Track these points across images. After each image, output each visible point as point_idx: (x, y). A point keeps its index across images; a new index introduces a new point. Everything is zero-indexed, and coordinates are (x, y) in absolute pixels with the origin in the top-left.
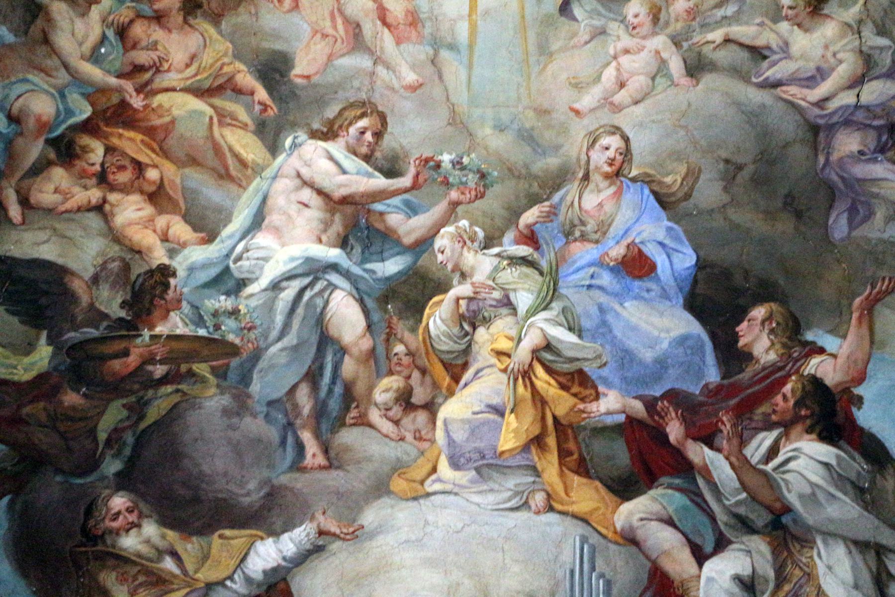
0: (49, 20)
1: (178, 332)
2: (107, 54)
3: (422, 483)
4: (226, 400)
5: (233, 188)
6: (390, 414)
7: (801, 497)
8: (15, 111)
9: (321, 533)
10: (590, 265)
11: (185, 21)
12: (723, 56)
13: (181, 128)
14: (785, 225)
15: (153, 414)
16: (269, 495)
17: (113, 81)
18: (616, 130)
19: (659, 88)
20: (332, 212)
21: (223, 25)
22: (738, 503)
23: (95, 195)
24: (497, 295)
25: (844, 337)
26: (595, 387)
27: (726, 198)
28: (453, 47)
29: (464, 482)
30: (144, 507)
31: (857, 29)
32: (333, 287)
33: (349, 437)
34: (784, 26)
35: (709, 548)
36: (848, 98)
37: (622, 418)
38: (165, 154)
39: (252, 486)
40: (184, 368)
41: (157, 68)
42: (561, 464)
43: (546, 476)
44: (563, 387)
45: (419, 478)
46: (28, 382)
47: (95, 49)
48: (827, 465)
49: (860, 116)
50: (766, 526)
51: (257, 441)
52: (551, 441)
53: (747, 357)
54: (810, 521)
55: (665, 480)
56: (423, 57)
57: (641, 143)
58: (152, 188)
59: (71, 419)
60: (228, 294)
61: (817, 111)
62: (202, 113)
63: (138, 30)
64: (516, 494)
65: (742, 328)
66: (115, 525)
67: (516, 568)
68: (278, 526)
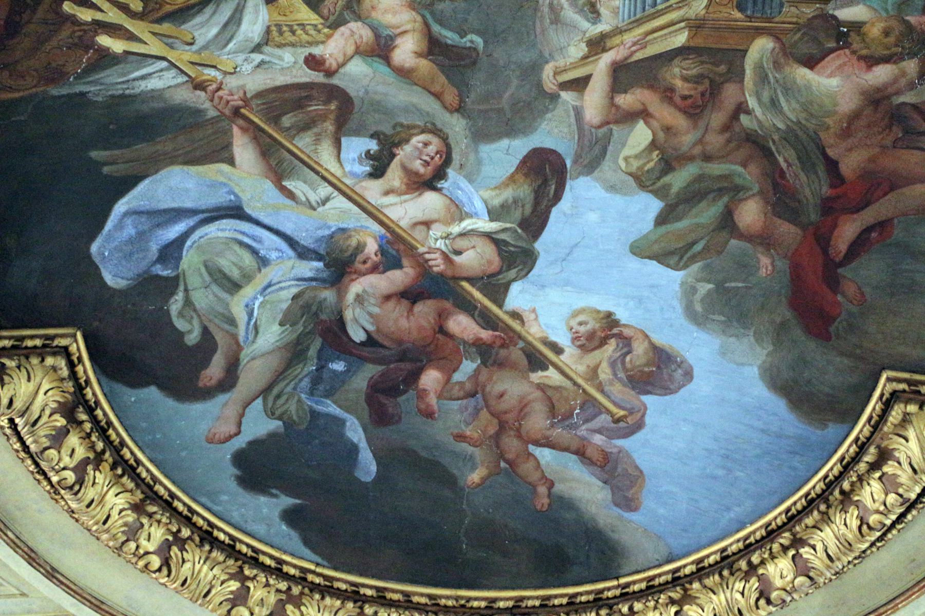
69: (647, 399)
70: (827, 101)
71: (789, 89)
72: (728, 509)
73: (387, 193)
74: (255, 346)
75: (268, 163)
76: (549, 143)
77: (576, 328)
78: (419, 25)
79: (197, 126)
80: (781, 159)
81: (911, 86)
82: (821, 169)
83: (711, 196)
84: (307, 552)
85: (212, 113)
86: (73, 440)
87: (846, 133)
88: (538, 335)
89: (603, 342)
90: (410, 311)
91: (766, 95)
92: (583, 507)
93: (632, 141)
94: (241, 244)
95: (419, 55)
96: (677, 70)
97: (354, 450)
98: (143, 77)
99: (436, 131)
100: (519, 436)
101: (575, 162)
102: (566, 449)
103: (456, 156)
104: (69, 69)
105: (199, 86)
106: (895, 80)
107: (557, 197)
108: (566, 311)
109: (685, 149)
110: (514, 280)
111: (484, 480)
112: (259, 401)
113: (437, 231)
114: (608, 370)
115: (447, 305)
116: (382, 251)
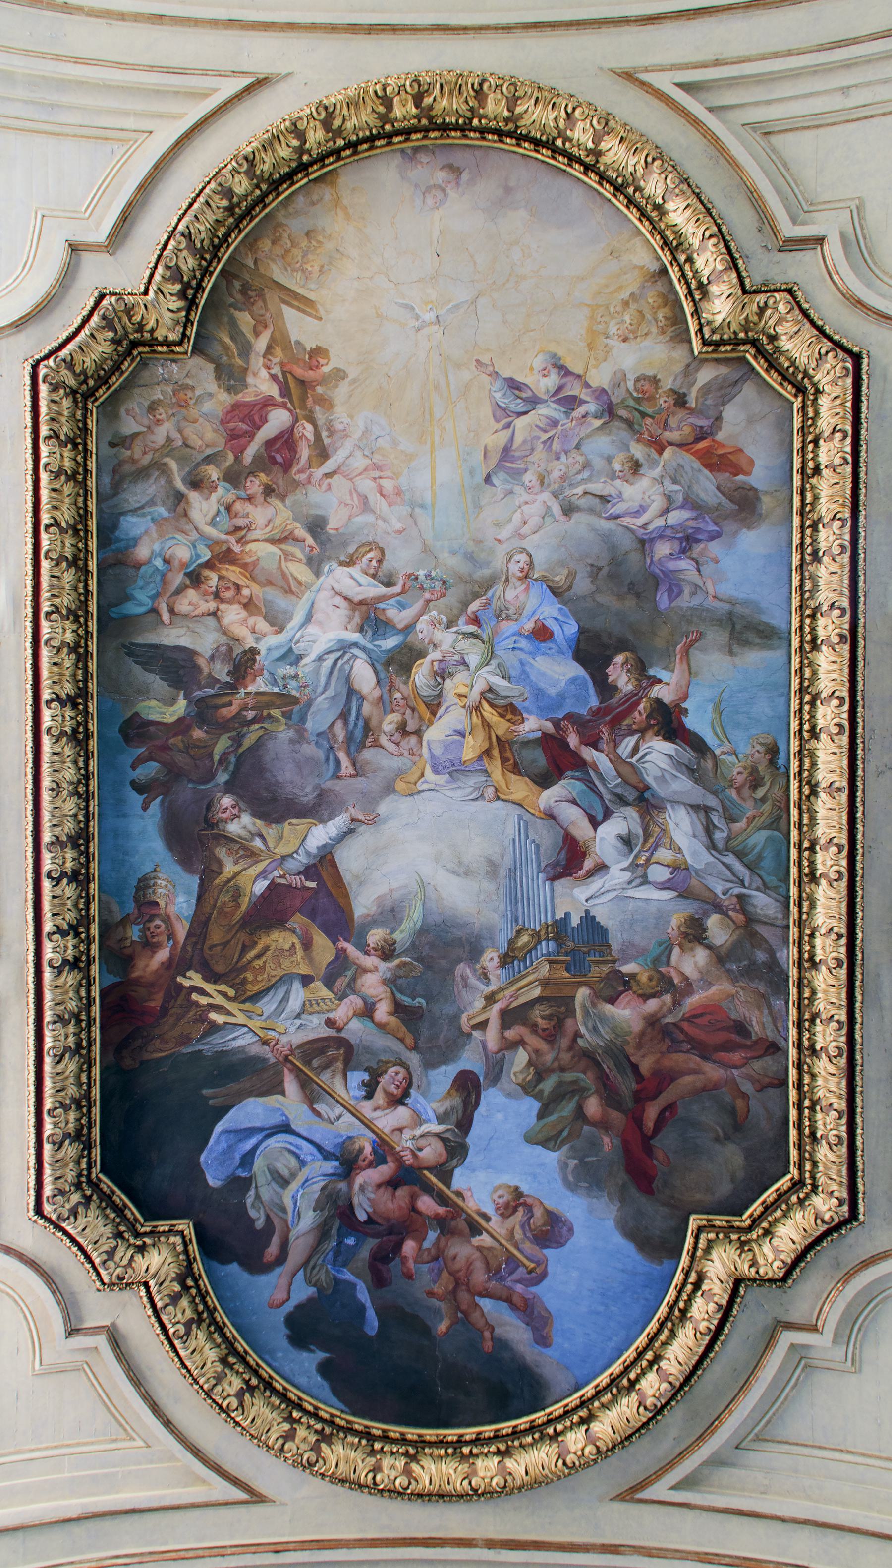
0: (188, 503)
1: (262, 690)
2: (220, 521)
3: (415, 784)
4: (291, 733)
5: (294, 598)
7: (655, 778)
8: (167, 556)
9: (353, 820)
10: (514, 635)
12: (583, 502)
13: (262, 563)
14: (630, 603)
15: (247, 742)
16: (319, 795)
17: (223, 537)
18: (523, 550)
20: (354, 610)
21: (287, 501)
22: (616, 786)
23: (212, 605)
24: (456, 657)
25: (673, 671)
26: (521, 715)
27: (594, 588)
28: (422, 506)
30: (242, 804)
32: (355, 657)
33: (368, 754)
34: (618, 482)
35: (600, 817)
36: (660, 522)
37: (539, 734)
38: (253, 579)
39: (308, 789)
40: (265, 713)
41: (248, 528)
42: (503, 767)
43: (493, 776)
44: (502, 716)
46: (172, 723)
47: (213, 518)
48: (669, 755)
49: (668, 533)
51: (311, 760)
52: (496, 752)
53: (615, 688)
55: (569, 773)
58: (246, 601)
59: (198, 747)
60: (291, 665)
61: (642, 531)
62: (274, 554)
63: (238, 506)
65: (610, 670)
66: (224, 816)
68: (325, 817)
69: (547, 1252)
70: (625, 1025)
71: (602, 1018)
72: (610, 1339)
73: (375, 1109)
75: (305, 1093)
76: (468, 1067)
77: (498, 1200)
78: (388, 994)
80: (605, 1067)
81: (670, 1011)
82: (629, 1071)
84: (334, 1400)
85: (273, 1060)
86: (184, 1302)
87: (639, 1046)
88: (475, 1208)
90: (393, 1195)
91: (590, 1025)
94: (290, 1151)
95: (390, 1014)
96: (537, 1012)
97: (362, 1309)
98: (234, 1039)
100: (469, 1291)
101: (485, 1078)
102: (499, 1298)
103: (415, 1080)
104: (193, 1036)
105: (265, 1043)
106: (661, 1008)
109: (548, 1064)
111: (449, 1328)
112: (301, 1272)
113: (407, 1134)
114: (520, 1232)
115: (416, 1189)
116: (374, 1151)
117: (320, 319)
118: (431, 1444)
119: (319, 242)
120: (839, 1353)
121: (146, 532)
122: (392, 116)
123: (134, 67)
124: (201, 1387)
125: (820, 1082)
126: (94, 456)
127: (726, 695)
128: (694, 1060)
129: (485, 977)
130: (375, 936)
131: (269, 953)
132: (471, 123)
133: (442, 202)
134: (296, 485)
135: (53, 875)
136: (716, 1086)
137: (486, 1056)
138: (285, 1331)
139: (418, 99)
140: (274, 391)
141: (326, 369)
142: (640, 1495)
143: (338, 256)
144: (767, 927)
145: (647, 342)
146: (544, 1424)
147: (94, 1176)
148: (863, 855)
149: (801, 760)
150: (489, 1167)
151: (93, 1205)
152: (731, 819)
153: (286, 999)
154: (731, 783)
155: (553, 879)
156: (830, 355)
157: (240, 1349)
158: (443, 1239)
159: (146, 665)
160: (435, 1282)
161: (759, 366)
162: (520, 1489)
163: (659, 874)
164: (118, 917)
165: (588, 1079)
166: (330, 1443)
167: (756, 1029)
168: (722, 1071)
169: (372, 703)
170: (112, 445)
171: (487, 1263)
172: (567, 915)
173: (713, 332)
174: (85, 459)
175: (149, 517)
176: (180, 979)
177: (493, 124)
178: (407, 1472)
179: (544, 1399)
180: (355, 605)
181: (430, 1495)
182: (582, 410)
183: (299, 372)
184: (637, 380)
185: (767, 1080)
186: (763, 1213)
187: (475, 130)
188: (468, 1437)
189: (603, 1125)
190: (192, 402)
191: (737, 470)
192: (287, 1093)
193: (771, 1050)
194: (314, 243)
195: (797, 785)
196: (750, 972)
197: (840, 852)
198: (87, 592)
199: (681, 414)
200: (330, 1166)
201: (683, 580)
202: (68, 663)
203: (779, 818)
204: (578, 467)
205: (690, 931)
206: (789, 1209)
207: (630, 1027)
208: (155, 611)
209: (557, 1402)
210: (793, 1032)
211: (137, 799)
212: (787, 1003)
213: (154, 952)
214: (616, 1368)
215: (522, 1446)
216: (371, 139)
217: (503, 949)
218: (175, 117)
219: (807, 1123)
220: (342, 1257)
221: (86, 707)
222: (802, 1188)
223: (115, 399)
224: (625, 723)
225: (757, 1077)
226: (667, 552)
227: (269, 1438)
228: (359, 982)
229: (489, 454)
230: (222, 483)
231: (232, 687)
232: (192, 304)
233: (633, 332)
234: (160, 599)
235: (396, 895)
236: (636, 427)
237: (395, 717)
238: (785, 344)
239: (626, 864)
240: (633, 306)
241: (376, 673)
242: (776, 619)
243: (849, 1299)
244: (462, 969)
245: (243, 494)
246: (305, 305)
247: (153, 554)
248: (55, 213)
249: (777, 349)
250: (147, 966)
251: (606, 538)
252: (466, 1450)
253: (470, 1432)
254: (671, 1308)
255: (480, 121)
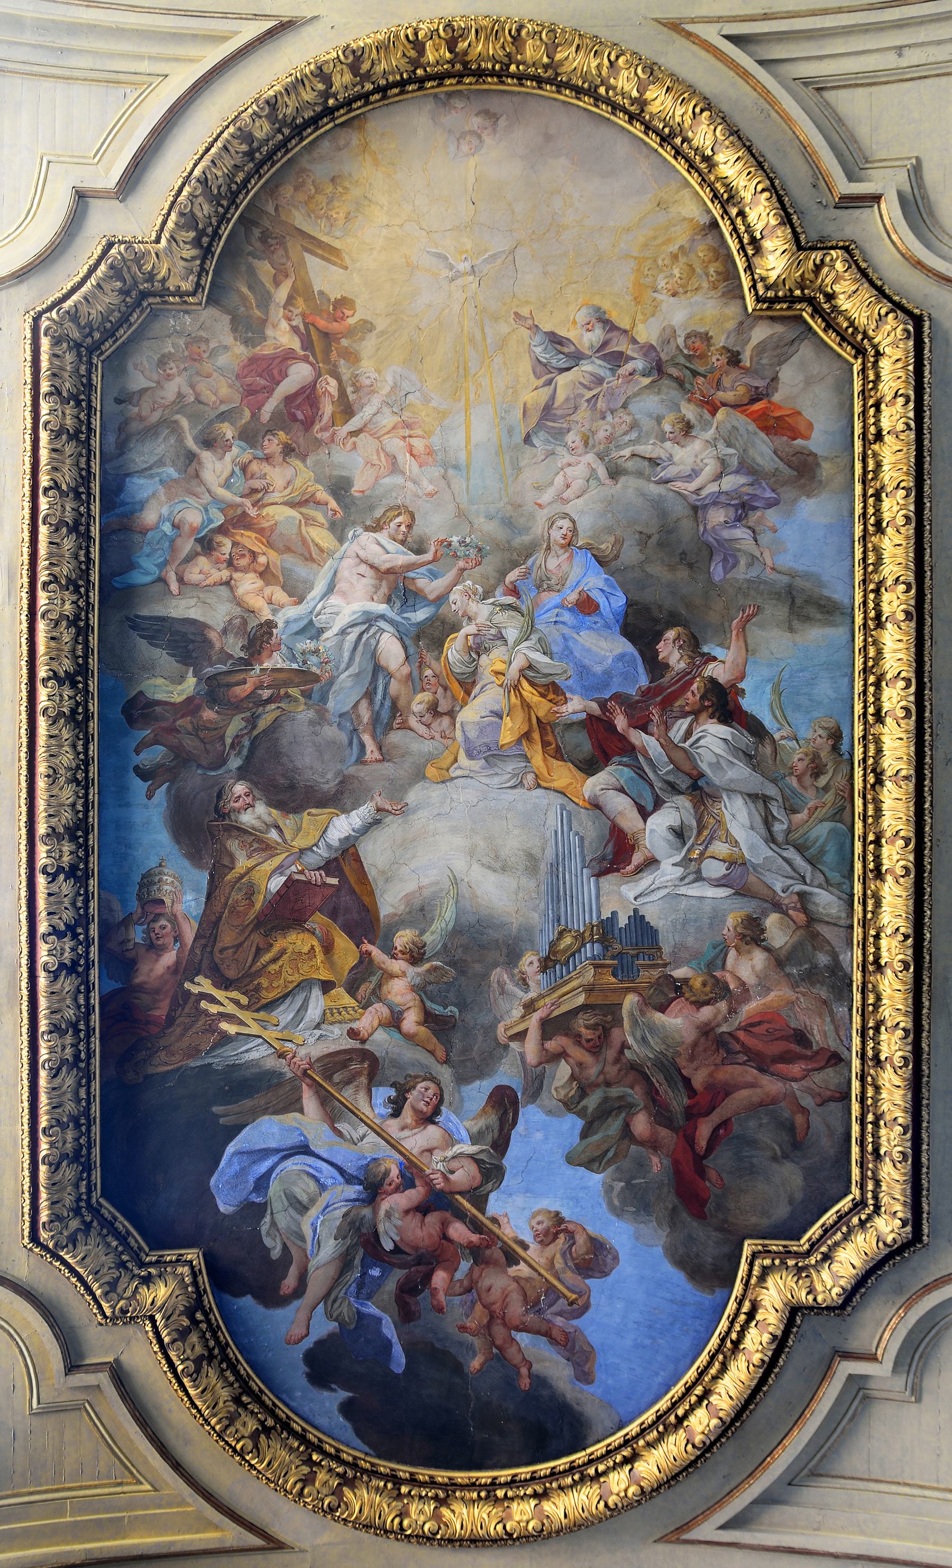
0: (200, 463)
1: (279, 666)
2: (235, 483)
3: (448, 770)
4: (311, 714)
5: (315, 566)
6: (424, 719)
7: (710, 764)
8: (176, 521)
9: (379, 810)
11: (284, 460)
12: (630, 465)
13: (280, 528)
14: (683, 573)
15: (262, 724)
16: (341, 782)
17: (238, 500)
18: (566, 516)
19: (592, 487)
20: (381, 579)
21: (309, 461)
22: (668, 773)
23: (225, 574)
24: (493, 631)
25: (728, 648)
27: (643, 557)
28: (456, 467)
29: (477, 768)
30: (257, 793)
31: (713, 443)
33: (395, 737)
34: (668, 444)
36: (713, 488)
37: (584, 716)
38: (270, 545)
40: (282, 692)
41: (266, 490)
43: (533, 761)
44: (543, 696)
45: (445, 766)
47: (227, 480)
49: (723, 499)
50: (688, 788)
51: (332, 743)
52: (536, 736)
53: (666, 666)
54: (717, 781)
55: (616, 759)
56: (437, 474)
57: (585, 524)
58: (262, 569)
60: (311, 639)
61: (695, 497)
62: (294, 518)
63: (255, 467)
64: (514, 775)
65: (660, 646)
66: (236, 805)
67: (516, 832)
68: (348, 807)
70: (677, 1037)
71: (652, 1029)
72: (657, 1374)
73: (403, 1129)
74: (319, 1257)
76: (505, 1082)
77: (537, 1227)
79: (279, 1085)
80: (654, 1080)
81: (726, 1020)
82: (680, 1085)
83: (614, 1113)
84: (358, 1442)
85: (289, 1075)
86: (194, 1338)
87: (692, 1058)
88: (511, 1235)
89: (555, 1237)
90: (423, 1221)
91: (638, 1035)
92: (554, 1383)
93: (558, 1076)
94: (309, 1174)
95: (419, 1023)
96: (581, 1021)
97: (388, 1344)
98: (247, 1051)
99: (433, 1079)
100: (505, 1325)
101: (523, 1094)
102: (538, 1333)
103: (446, 1097)
104: (202, 1048)
105: (281, 1055)
106: (715, 1016)
107: (515, 1123)
108: (527, 1213)
109: (593, 1078)
110: (491, 1191)
111: (482, 1365)
112: (321, 1305)
113: (438, 1155)
115: (448, 1215)
116: (402, 1174)
117: (346, 268)
118: (462, 1487)
119: (345, 188)
120: (899, 1383)
121: (154, 495)
122: (423, 60)
123: (150, 10)
124: (213, 1428)
125: (884, 1095)
126: (98, 414)
127: (786, 675)
128: (751, 1073)
129: (524, 983)
130: (403, 938)
131: (285, 957)
132: (508, 68)
133: (478, 149)
134: (318, 443)
135: (49, 870)
136: (774, 1101)
137: (525, 1069)
138: (303, 1368)
139: (451, 45)
140: (296, 344)
141: (351, 321)
142: (686, 1536)
143: (366, 203)
144: (831, 927)
145: (698, 298)
146: (584, 1464)
147: (94, 1200)
148: (931, 849)
149: (865, 746)
150: (527, 1191)
151: (93, 1232)
152: (792, 810)
153: (304, 1007)
154: (791, 770)
155: (599, 875)
156: (891, 316)
157: (256, 1388)
158: (476, 1269)
159: (152, 639)
160: (467, 1316)
161: (817, 326)
162: (558, 1532)
163: (714, 869)
164: (120, 916)
165: (636, 1094)
166: (352, 1487)
167: (817, 1038)
168: (780, 1084)
169: (400, 681)
170: (119, 401)
171: (525, 1295)
172: (614, 914)
173: (767, 288)
174: (89, 416)
175: (157, 479)
176: (187, 985)
177: (531, 70)
178: (437, 1516)
179: (585, 1438)
180: (382, 574)
181: (461, 1540)
182: (629, 366)
183: (322, 323)
184: (688, 337)
185: (829, 1093)
186: (822, 1237)
187: (512, 76)
188: (502, 1480)
189: (653, 1145)
190: (205, 355)
191: (795, 434)
192: (306, 1110)
193: (833, 1061)
194: (340, 189)
195: (861, 773)
196: (811, 976)
197: (907, 846)
198: (89, 560)
199: (735, 373)
200: (353, 1191)
201: (739, 550)
202: (66, 638)
203: (842, 809)
204: (624, 427)
205: (748, 932)
206: (850, 1231)
207: (682, 1037)
208: (162, 580)
209: (599, 1441)
210: (856, 1041)
211: (139, 786)
212: (851, 1010)
213: (159, 956)
214: (663, 1404)
215: (561, 1488)
216: (402, 84)
217: (544, 952)
218: (192, 61)
219: (870, 1140)
220: (365, 1289)
221: (87, 685)
222: (864, 1209)
223: (122, 352)
224: (677, 704)
225: (817, 1090)
226: (722, 519)
227: (286, 1482)
228: (385, 989)
229: (528, 413)
230: (237, 442)
231: (247, 663)
232: (207, 252)
233: (681, 286)
234: (168, 568)
235: (426, 893)
236: (687, 386)
237: (426, 697)
238: (843, 303)
239: (678, 858)
240: (682, 260)
241: (405, 648)
242: (838, 594)
243: (910, 1326)
244: (499, 974)
245: (260, 453)
246: (330, 254)
247: (161, 520)
248: (61, 159)
249: (835, 308)
250: (151, 970)
251: (658, 505)
252: (500, 1493)
253: (505, 1474)
254: (723, 1340)
255: (518, 67)
